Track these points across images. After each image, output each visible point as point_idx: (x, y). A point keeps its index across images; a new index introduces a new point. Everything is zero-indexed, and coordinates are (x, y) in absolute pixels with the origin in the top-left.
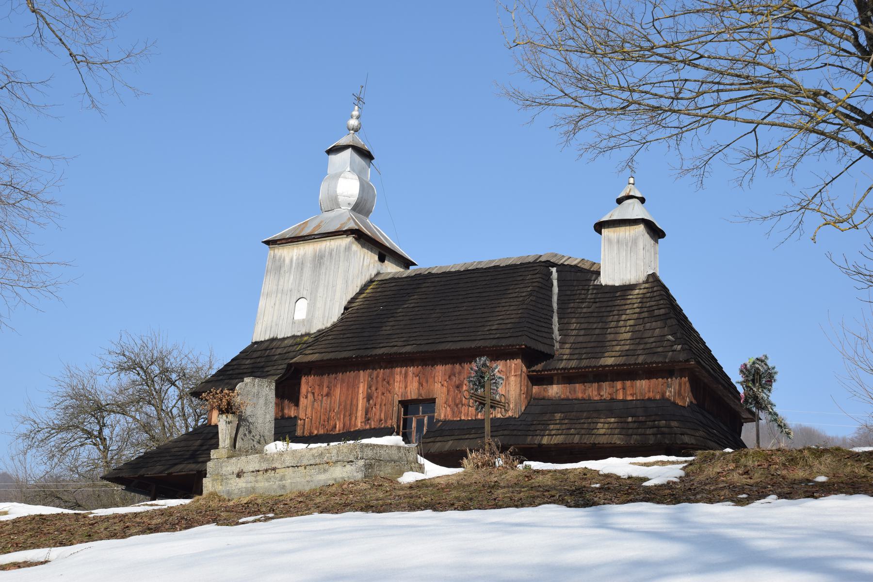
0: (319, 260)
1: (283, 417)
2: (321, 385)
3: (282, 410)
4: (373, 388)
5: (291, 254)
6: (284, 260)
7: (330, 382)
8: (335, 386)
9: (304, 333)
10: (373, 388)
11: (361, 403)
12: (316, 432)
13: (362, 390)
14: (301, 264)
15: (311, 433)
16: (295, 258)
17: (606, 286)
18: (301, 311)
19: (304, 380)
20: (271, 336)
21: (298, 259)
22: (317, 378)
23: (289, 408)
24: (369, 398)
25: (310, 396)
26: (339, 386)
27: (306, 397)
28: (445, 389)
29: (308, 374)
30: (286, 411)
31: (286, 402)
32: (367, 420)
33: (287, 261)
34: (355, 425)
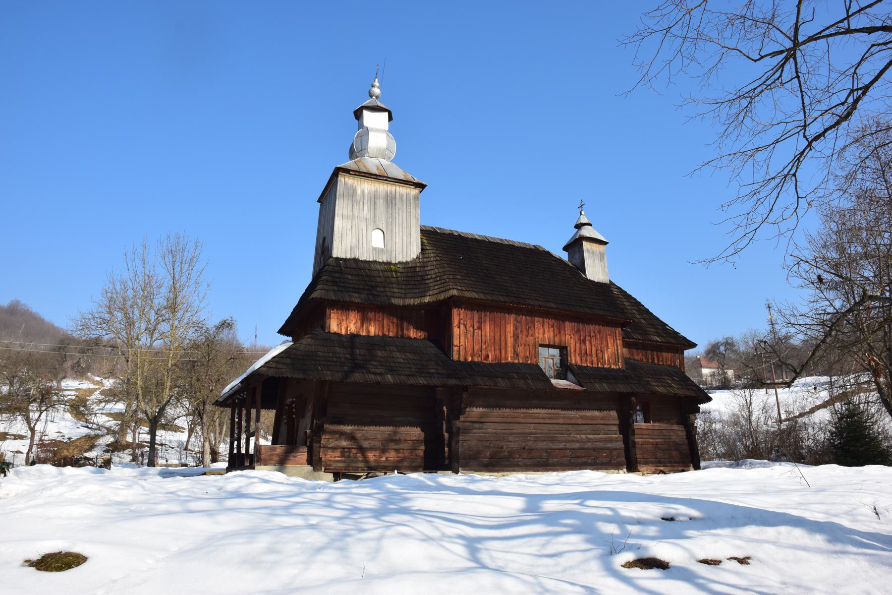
0: (390, 200)
1: (402, 336)
2: (472, 319)
3: (402, 330)
4: (519, 331)
5: (362, 187)
6: (355, 190)
7: (480, 318)
8: (485, 322)
9: (385, 261)
10: (519, 331)
11: (510, 341)
12: (470, 359)
13: (510, 329)
14: (374, 197)
15: (466, 359)
16: (366, 192)
17: (590, 280)
18: (377, 240)
19: (455, 311)
20: (353, 256)
21: (370, 193)
22: (469, 313)
23: (408, 329)
24: (516, 337)
25: (462, 327)
26: (488, 323)
27: (459, 327)
28: (572, 341)
29: (459, 306)
30: (405, 332)
31: (405, 324)
32: (516, 354)
33: (359, 192)
34: (506, 358)
